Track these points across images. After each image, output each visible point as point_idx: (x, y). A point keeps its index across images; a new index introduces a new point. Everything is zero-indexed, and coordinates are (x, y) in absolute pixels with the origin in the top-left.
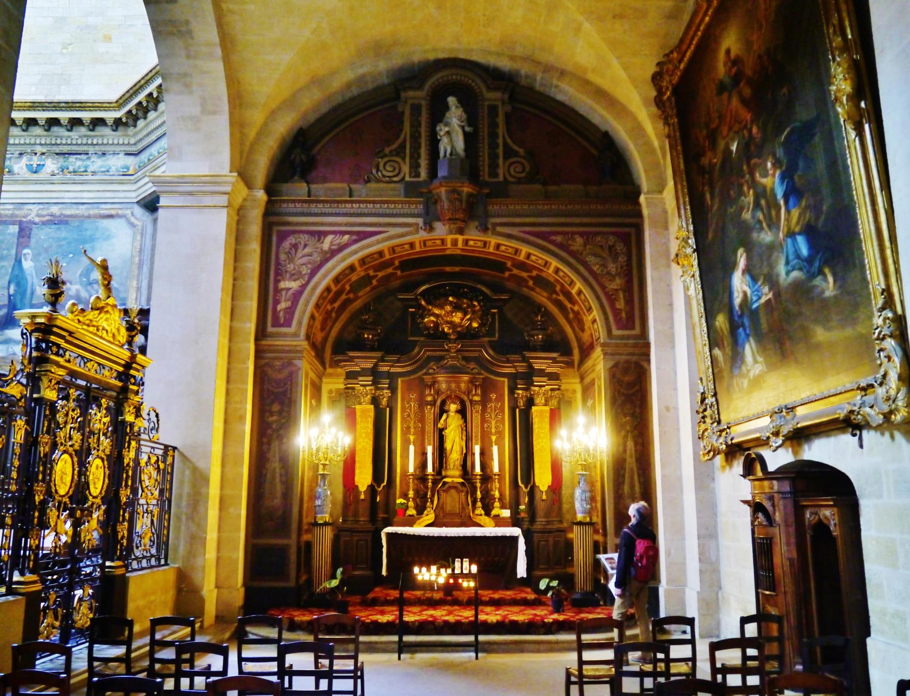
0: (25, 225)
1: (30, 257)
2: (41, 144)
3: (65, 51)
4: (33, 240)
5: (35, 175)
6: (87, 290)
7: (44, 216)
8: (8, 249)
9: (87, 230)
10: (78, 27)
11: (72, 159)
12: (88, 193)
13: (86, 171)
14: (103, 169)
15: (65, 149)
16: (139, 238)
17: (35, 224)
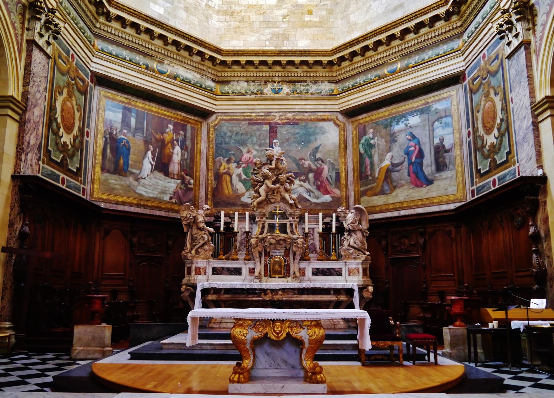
0: (273, 125)
1: (278, 144)
2: (279, 76)
3: (284, 20)
4: (279, 134)
5: (277, 95)
6: (314, 164)
7: (284, 120)
8: (264, 140)
9: (311, 128)
10: (292, 5)
11: (298, 85)
12: (309, 106)
13: (307, 93)
14: (318, 91)
15: (293, 79)
16: (342, 133)
17: (279, 124)
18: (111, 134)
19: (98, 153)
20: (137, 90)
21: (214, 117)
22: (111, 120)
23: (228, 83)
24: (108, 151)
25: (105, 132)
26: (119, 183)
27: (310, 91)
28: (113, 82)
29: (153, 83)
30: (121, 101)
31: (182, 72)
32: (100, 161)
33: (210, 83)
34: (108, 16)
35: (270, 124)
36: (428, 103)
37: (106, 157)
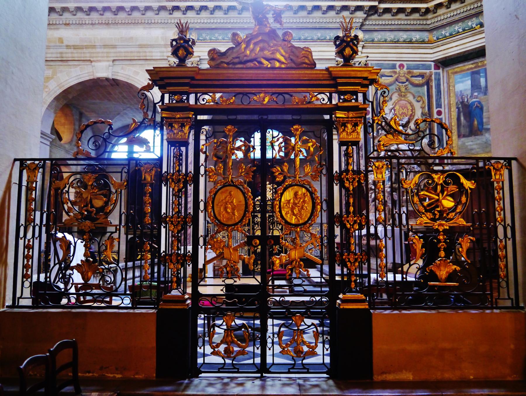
18: (462, 103)
19: (453, 124)
20: (478, 51)
22: (461, 91)
24: (462, 118)
25: (457, 103)
26: (475, 143)
28: (455, 58)
29: (456, 46)
30: (468, 69)
32: (456, 129)
37: (461, 124)
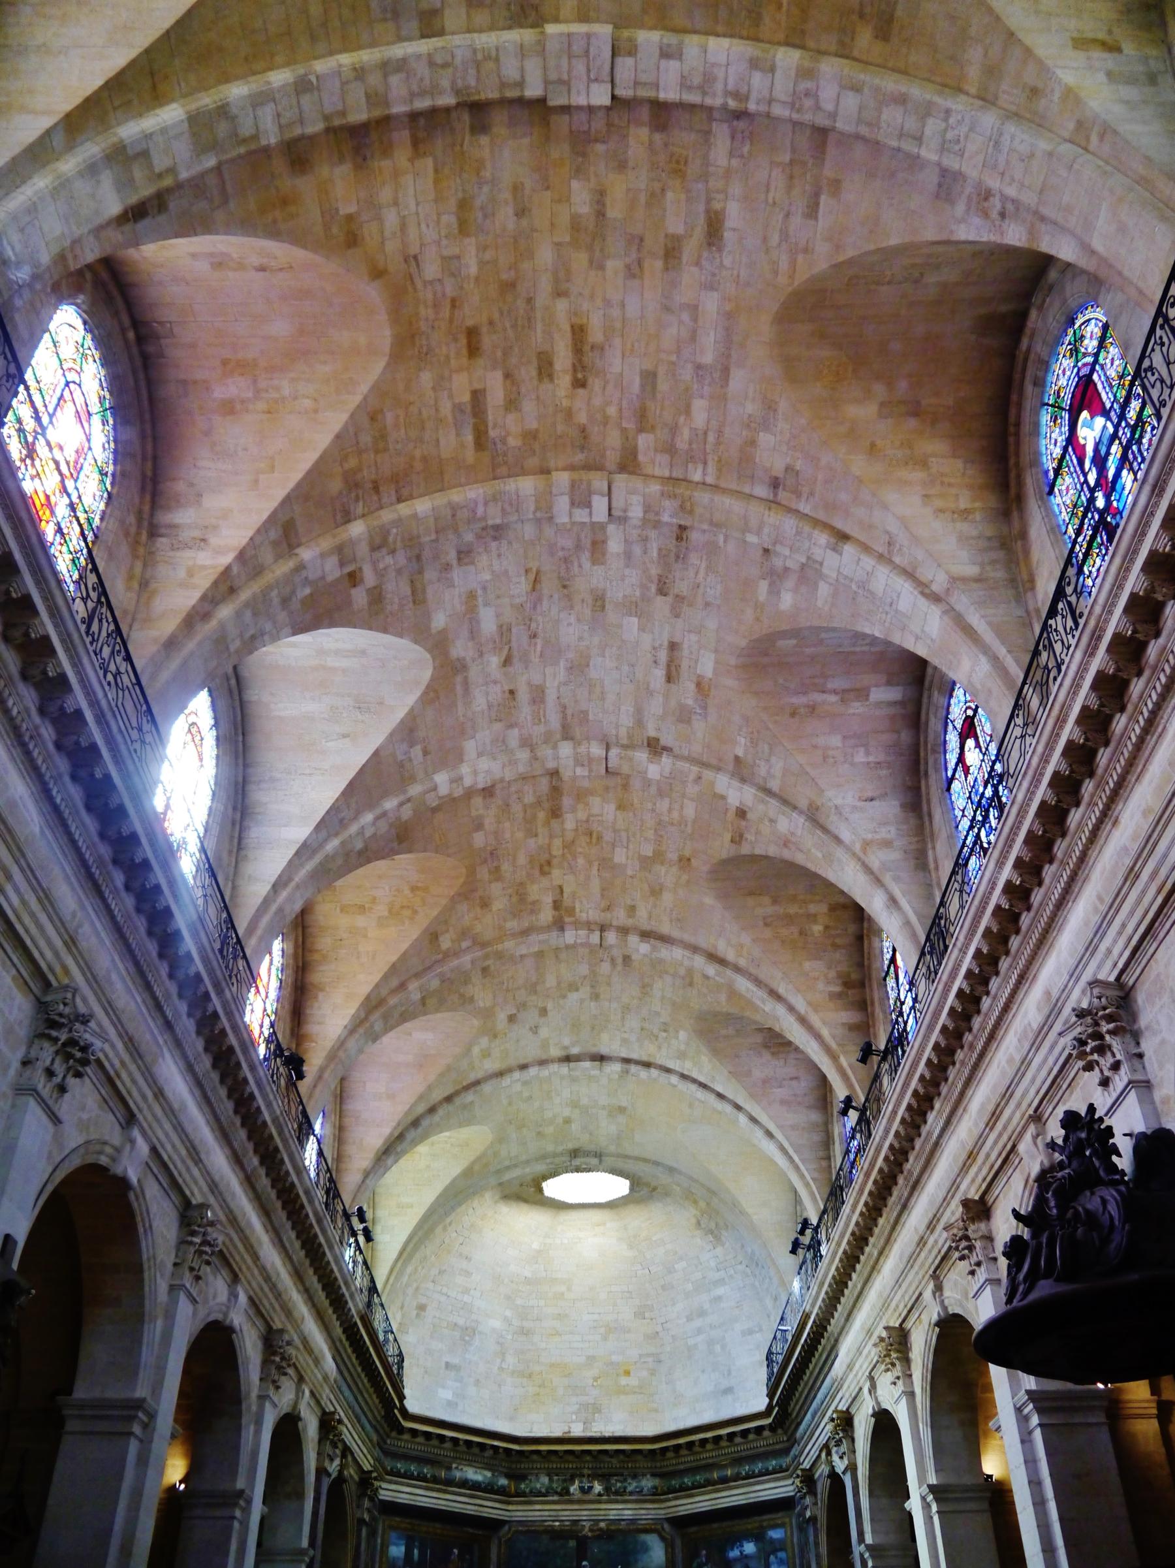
15: (606, 1471)
21: (507, 1528)
23: (522, 1477)
27: (630, 1489)
31: (473, 1474)
33: (503, 1481)
34: (401, 1430)
35: (577, 1538)
36: (761, 1527)
